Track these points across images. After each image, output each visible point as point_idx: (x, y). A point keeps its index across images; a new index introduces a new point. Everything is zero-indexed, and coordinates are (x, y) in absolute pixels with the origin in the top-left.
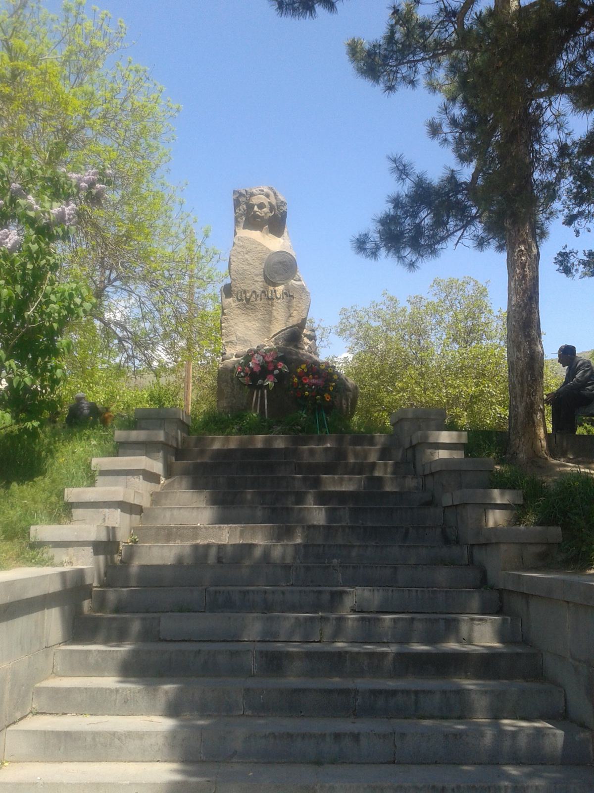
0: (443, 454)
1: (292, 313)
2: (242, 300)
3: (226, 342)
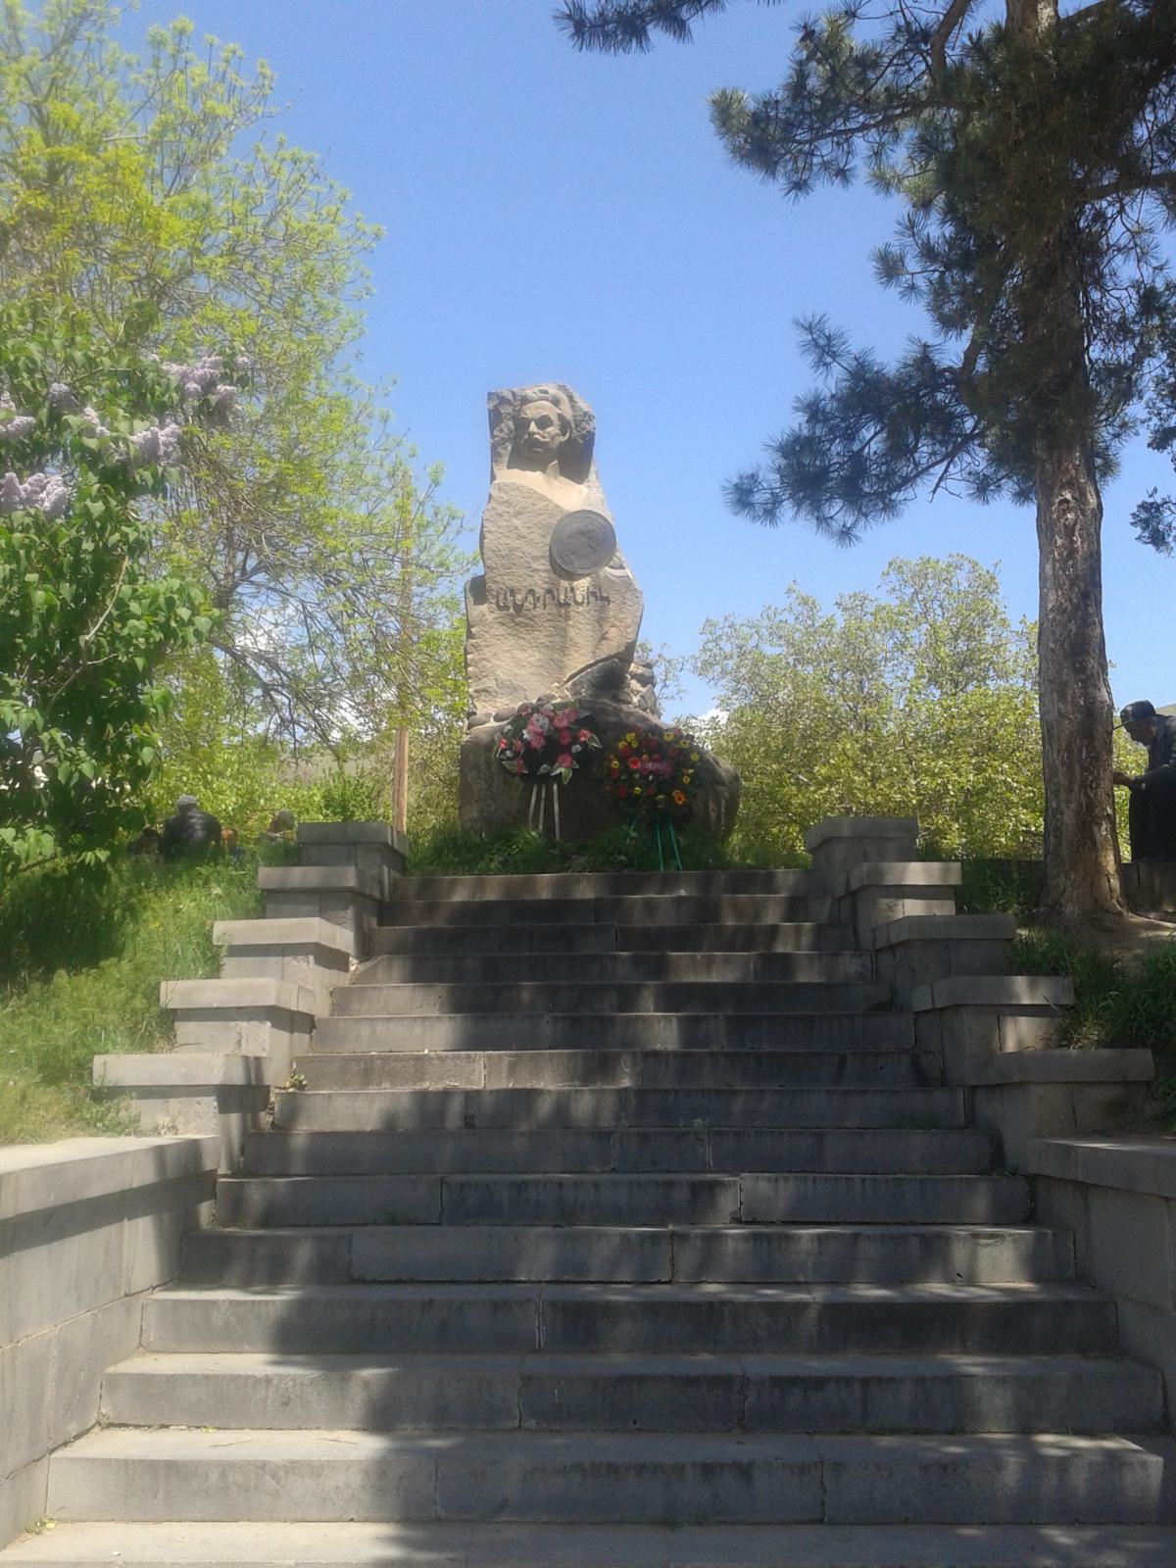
0: (912, 908)
2: (506, 607)
3: (476, 691)
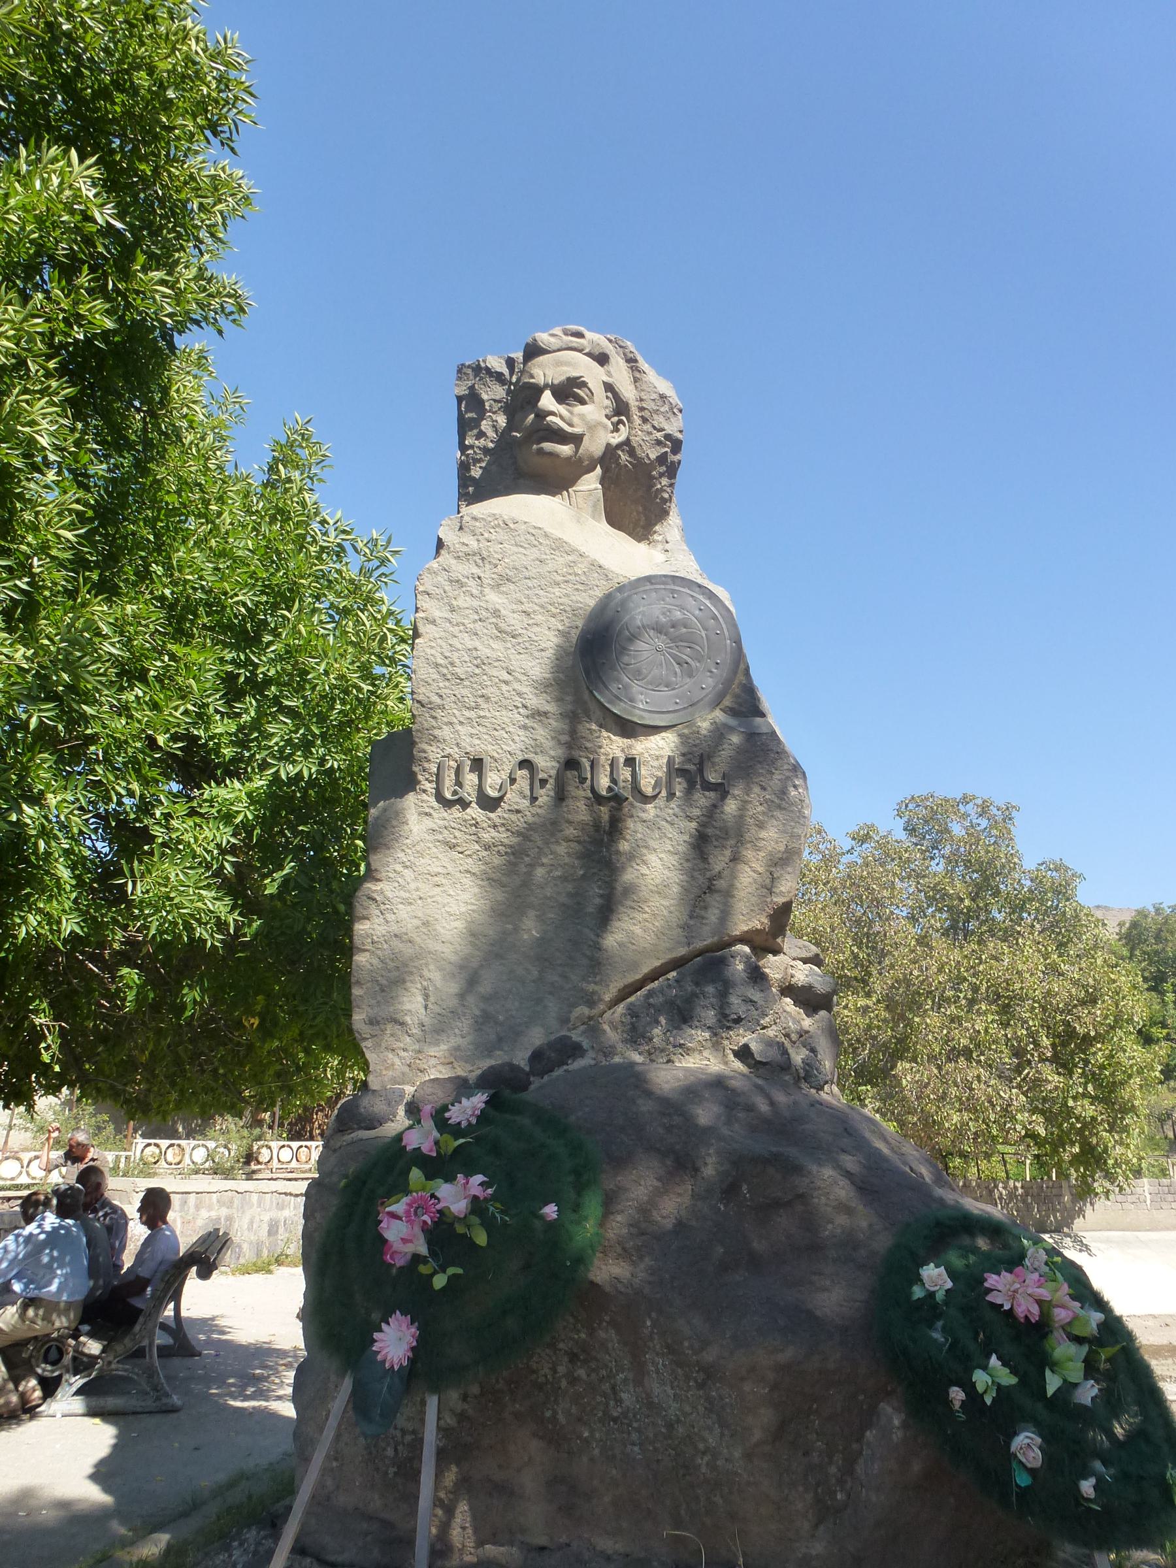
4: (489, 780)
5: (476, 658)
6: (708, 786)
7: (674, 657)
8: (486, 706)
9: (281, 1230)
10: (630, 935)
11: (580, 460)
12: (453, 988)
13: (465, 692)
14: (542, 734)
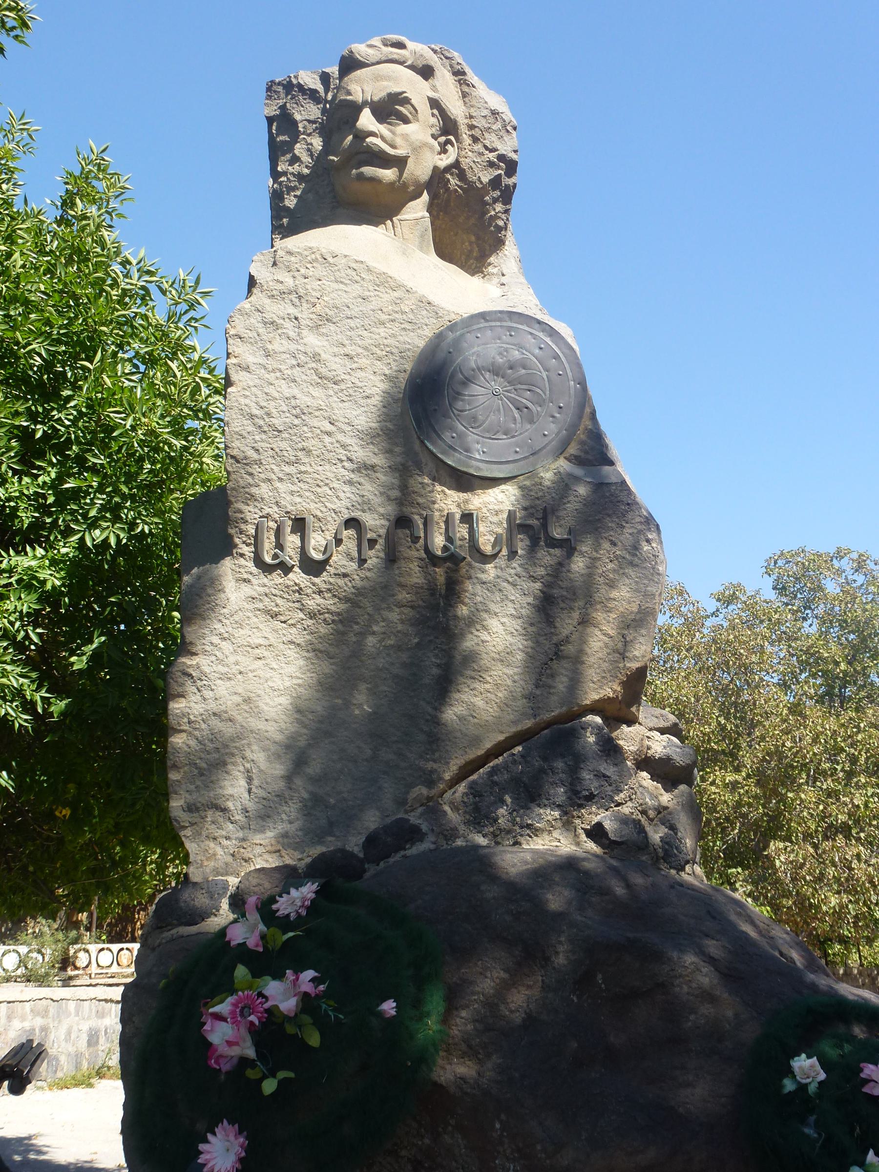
1: (567, 640)
4: (313, 542)
5: (294, 408)
6: (553, 543)
7: (513, 401)
8: (306, 460)
9: (102, 1040)
10: (472, 707)
11: (405, 185)
12: (279, 769)
13: (284, 445)
14: (369, 489)
